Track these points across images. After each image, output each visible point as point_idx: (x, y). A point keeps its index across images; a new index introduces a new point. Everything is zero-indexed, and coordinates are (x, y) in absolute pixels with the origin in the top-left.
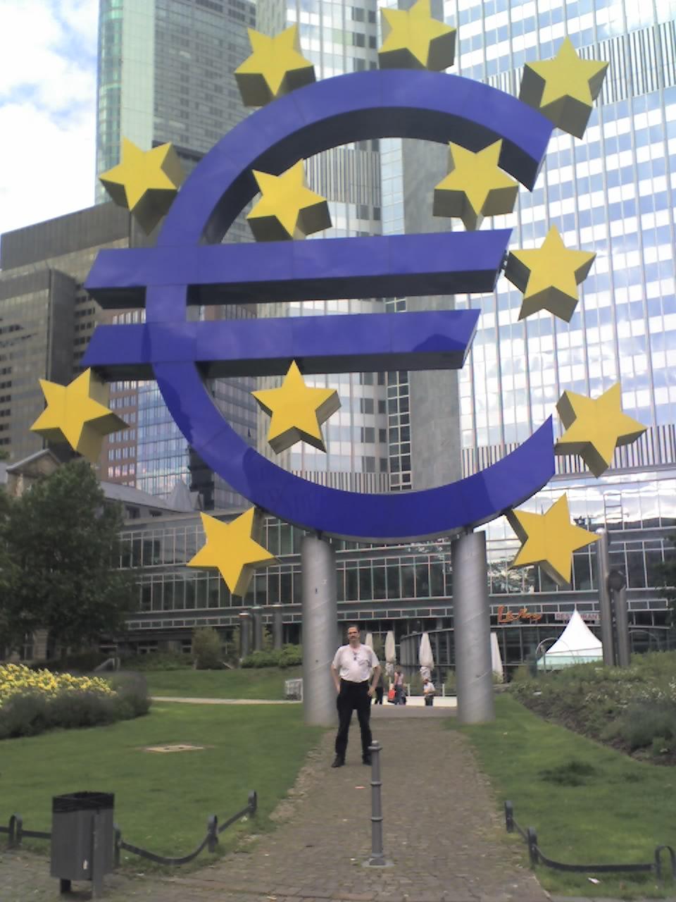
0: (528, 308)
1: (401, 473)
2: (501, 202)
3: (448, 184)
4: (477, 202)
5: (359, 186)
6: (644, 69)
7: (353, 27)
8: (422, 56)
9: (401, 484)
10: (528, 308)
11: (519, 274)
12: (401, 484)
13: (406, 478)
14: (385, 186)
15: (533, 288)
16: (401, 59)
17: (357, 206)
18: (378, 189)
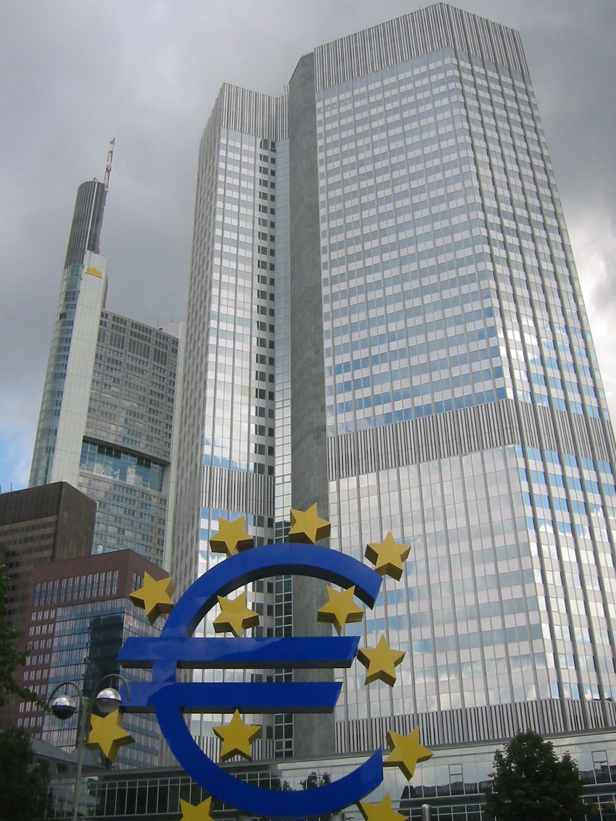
0: (369, 680)
1: (284, 740)
2: (355, 617)
3: (324, 610)
4: (341, 618)
5: (257, 501)
6: (469, 436)
7: (256, 384)
8: (312, 536)
9: (284, 749)
10: (369, 680)
11: (365, 661)
12: (284, 749)
13: (289, 745)
14: (278, 502)
15: (374, 669)
16: (302, 538)
17: (255, 516)
18: (272, 504)
